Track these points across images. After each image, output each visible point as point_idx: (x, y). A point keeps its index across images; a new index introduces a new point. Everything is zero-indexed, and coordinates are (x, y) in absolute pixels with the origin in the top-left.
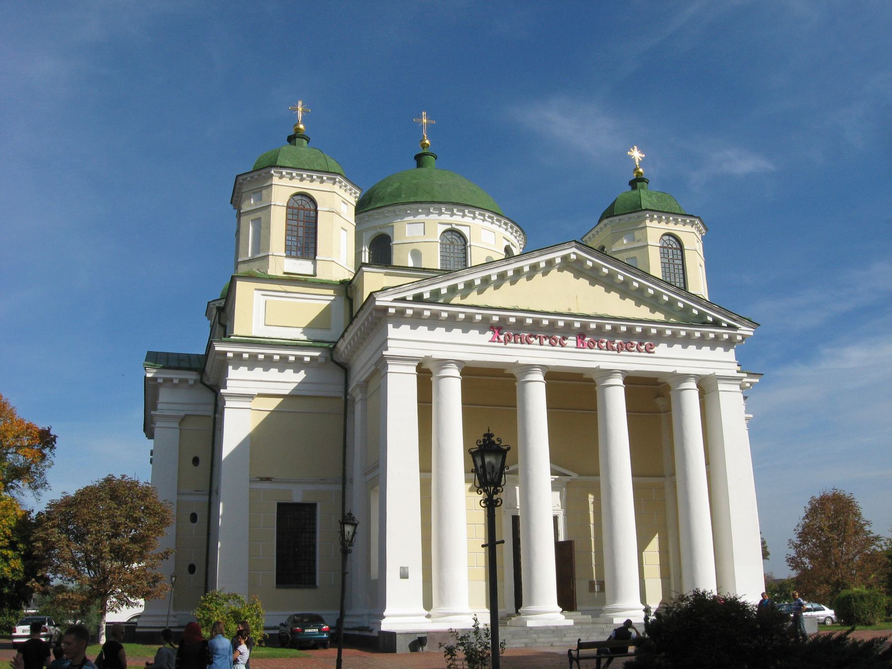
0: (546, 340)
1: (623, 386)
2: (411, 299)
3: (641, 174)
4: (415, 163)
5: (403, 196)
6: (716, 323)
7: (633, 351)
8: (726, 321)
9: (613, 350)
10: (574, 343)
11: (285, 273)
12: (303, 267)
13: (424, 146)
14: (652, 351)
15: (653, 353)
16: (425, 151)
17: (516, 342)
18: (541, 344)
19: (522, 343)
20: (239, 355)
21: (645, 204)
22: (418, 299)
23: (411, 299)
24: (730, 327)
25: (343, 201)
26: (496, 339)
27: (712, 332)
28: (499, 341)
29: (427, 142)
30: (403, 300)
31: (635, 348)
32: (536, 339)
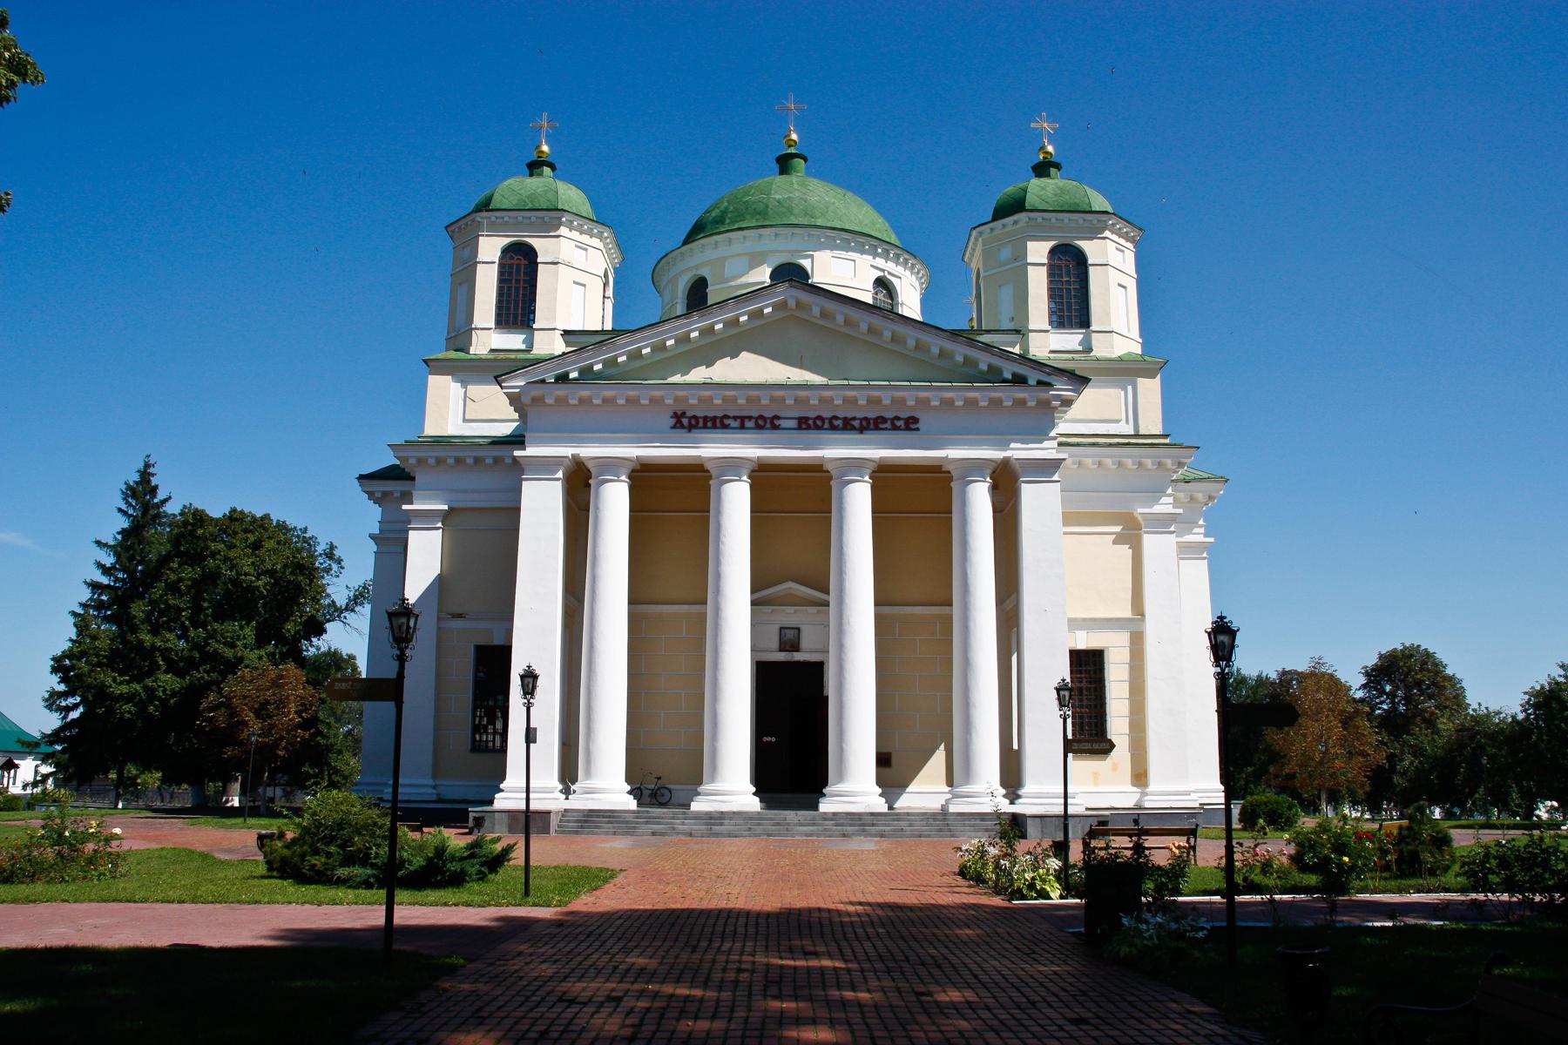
0: (750, 420)
1: (869, 482)
2: (553, 380)
3: (1051, 154)
4: (776, 167)
5: (728, 221)
6: (1019, 380)
7: (886, 429)
8: (1033, 377)
9: (853, 428)
10: (793, 424)
11: (492, 351)
12: (513, 341)
13: (791, 143)
14: (913, 426)
15: (917, 429)
16: (793, 150)
17: (705, 427)
18: (742, 427)
19: (714, 427)
20: (421, 461)
21: (1031, 200)
22: (563, 378)
23: (553, 380)
24: (1040, 383)
25: (577, 246)
26: (678, 425)
27: (1008, 395)
28: (683, 427)
29: (794, 136)
30: (543, 381)
31: (888, 425)
32: (735, 420)
